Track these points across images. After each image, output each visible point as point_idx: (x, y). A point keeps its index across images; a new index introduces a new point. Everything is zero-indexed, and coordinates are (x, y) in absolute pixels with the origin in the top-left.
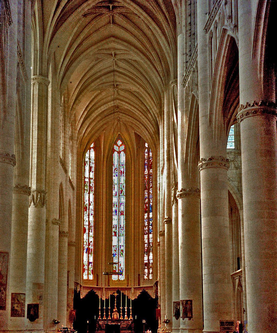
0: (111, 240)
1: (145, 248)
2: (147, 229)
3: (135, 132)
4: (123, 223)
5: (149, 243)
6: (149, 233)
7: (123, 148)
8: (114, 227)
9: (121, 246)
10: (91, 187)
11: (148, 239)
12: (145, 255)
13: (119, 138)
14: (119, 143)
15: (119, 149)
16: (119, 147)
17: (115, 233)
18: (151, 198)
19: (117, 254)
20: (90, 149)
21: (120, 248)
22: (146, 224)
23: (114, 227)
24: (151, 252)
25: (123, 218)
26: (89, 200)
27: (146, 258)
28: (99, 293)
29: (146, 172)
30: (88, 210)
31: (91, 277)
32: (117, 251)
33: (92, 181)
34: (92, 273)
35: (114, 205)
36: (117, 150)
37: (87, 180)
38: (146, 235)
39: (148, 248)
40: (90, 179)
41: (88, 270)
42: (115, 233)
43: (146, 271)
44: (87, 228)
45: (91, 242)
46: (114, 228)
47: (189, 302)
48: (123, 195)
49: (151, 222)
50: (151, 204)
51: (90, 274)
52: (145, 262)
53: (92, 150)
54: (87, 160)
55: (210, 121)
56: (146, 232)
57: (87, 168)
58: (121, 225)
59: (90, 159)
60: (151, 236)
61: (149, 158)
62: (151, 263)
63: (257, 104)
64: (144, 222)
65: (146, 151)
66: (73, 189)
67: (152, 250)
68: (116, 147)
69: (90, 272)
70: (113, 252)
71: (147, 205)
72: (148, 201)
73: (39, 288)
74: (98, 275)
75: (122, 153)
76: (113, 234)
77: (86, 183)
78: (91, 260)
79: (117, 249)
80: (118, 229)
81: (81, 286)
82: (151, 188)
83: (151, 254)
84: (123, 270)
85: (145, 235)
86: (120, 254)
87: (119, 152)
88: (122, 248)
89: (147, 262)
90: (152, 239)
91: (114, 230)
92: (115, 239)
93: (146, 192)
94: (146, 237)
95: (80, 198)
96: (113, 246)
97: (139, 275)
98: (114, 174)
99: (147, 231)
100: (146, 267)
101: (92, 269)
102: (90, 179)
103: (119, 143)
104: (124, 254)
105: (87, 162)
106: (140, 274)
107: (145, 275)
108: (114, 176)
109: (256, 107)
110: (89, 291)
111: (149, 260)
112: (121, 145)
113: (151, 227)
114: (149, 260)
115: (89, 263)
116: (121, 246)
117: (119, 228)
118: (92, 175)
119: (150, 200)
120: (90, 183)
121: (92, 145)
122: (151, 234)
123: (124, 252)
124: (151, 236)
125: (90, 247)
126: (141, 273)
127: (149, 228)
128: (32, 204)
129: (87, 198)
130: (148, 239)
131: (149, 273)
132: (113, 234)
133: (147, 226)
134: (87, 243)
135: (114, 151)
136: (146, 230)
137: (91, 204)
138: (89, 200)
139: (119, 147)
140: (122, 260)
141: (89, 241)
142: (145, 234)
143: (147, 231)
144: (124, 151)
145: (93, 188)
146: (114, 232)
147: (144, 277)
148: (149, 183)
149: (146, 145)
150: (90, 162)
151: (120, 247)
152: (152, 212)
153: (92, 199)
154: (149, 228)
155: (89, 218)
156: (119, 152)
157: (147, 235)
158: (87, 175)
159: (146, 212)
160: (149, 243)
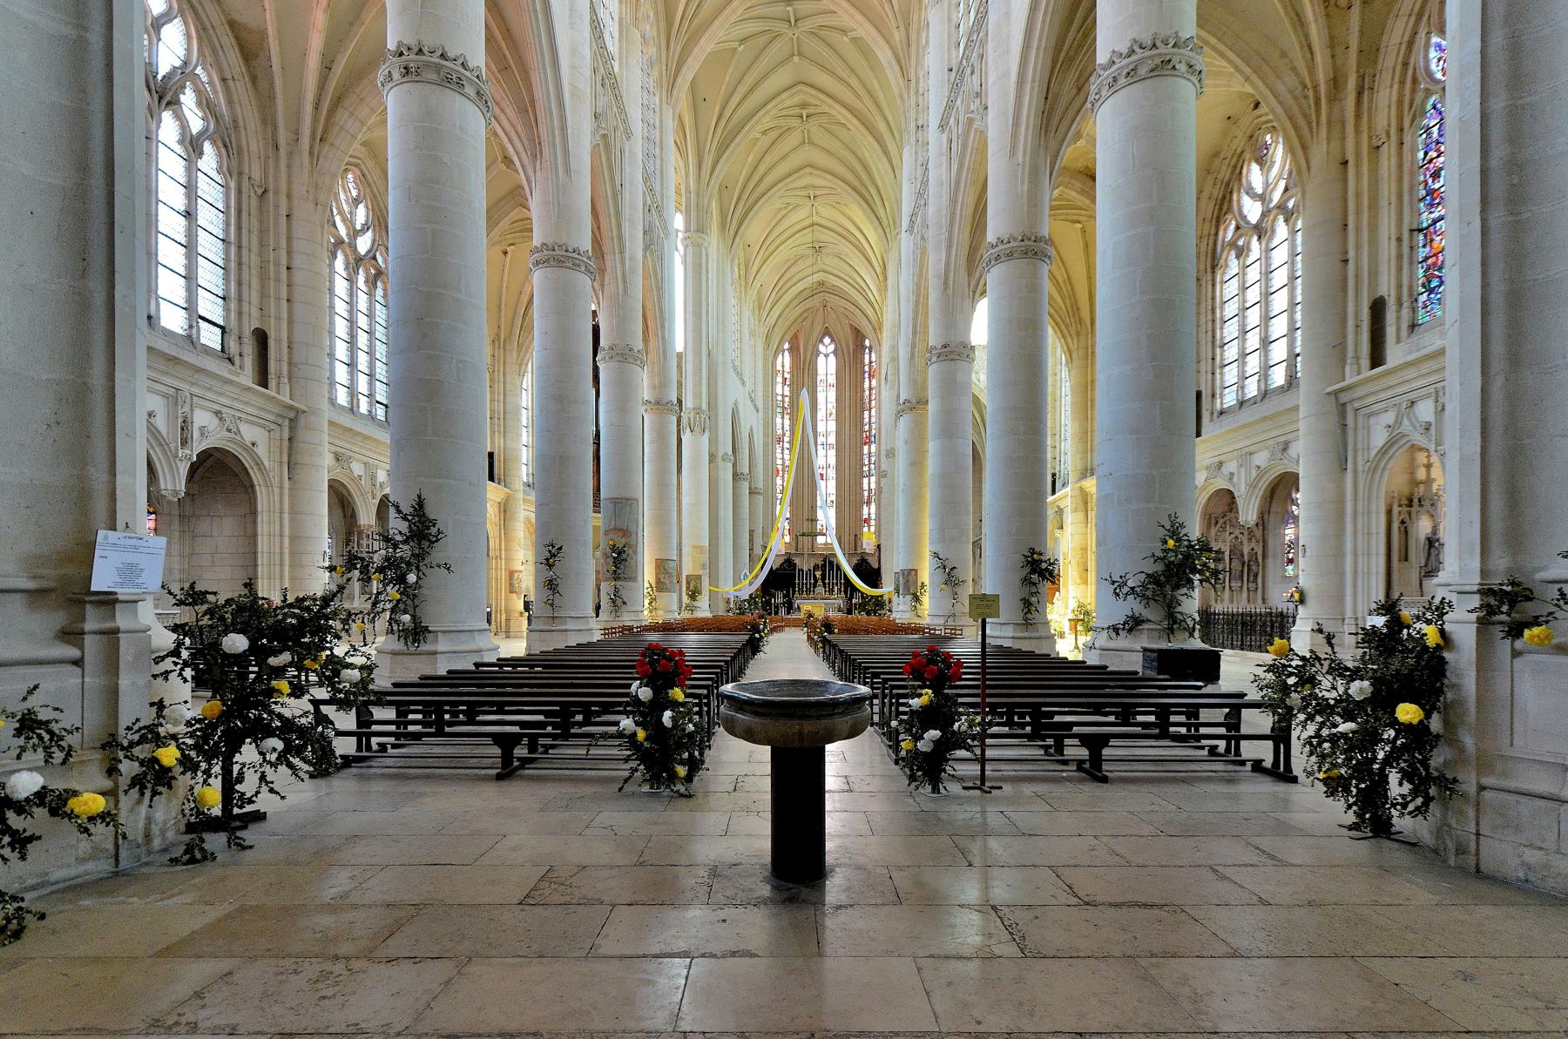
3: (851, 325)
4: (832, 461)
5: (870, 490)
6: (869, 476)
11: (869, 483)
12: (865, 507)
13: (827, 332)
14: (827, 340)
17: (822, 475)
20: (783, 351)
22: (867, 462)
25: (832, 453)
26: (783, 428)
28: (797, 561)
29: (866, 385)
31: (787, 539)
33: (787, 399)
37: (780, 398)
39: (869, 496)
40: (783, 396)
43: (866, 529)
44: (780, 467)
47: (913, 573)
49: (873, 459)
50: (874, 432)
53: (786, 354)
54: (779, 367)
55: (946, 283)
57: (779, 379)
59: (783, 366)
60: (873, 479)
61: (871, 362)
63: (1015, 239)
65: (867, 351)
66: (758, 410)
68: (822, 348)
69: (786, 532)
73: (701, 553)
75: (832, 355)
83: (873, 506)
87: (827, 356)
94: (865, 480)
95: (769, 425)
98: (819, 389)
102: (783, 396)
103: (827, 340)
109: (1013, 244)
111: (869, 514)
114: (869, 514)
118: (787, 392)
120: (783, 401)
121: (786, 346)
124: (873, 479)
126: (858, 533)
128: (688, 429)
129: (779, 426)
130: (869, 483)
135: (818, 353)
138: (783, 428)
140: (832, 513)
148: (870, 401)
149: (867, 343)
153: (787, 427)
156: (827, 356)
158: (779, 389)
160: (870, 490)
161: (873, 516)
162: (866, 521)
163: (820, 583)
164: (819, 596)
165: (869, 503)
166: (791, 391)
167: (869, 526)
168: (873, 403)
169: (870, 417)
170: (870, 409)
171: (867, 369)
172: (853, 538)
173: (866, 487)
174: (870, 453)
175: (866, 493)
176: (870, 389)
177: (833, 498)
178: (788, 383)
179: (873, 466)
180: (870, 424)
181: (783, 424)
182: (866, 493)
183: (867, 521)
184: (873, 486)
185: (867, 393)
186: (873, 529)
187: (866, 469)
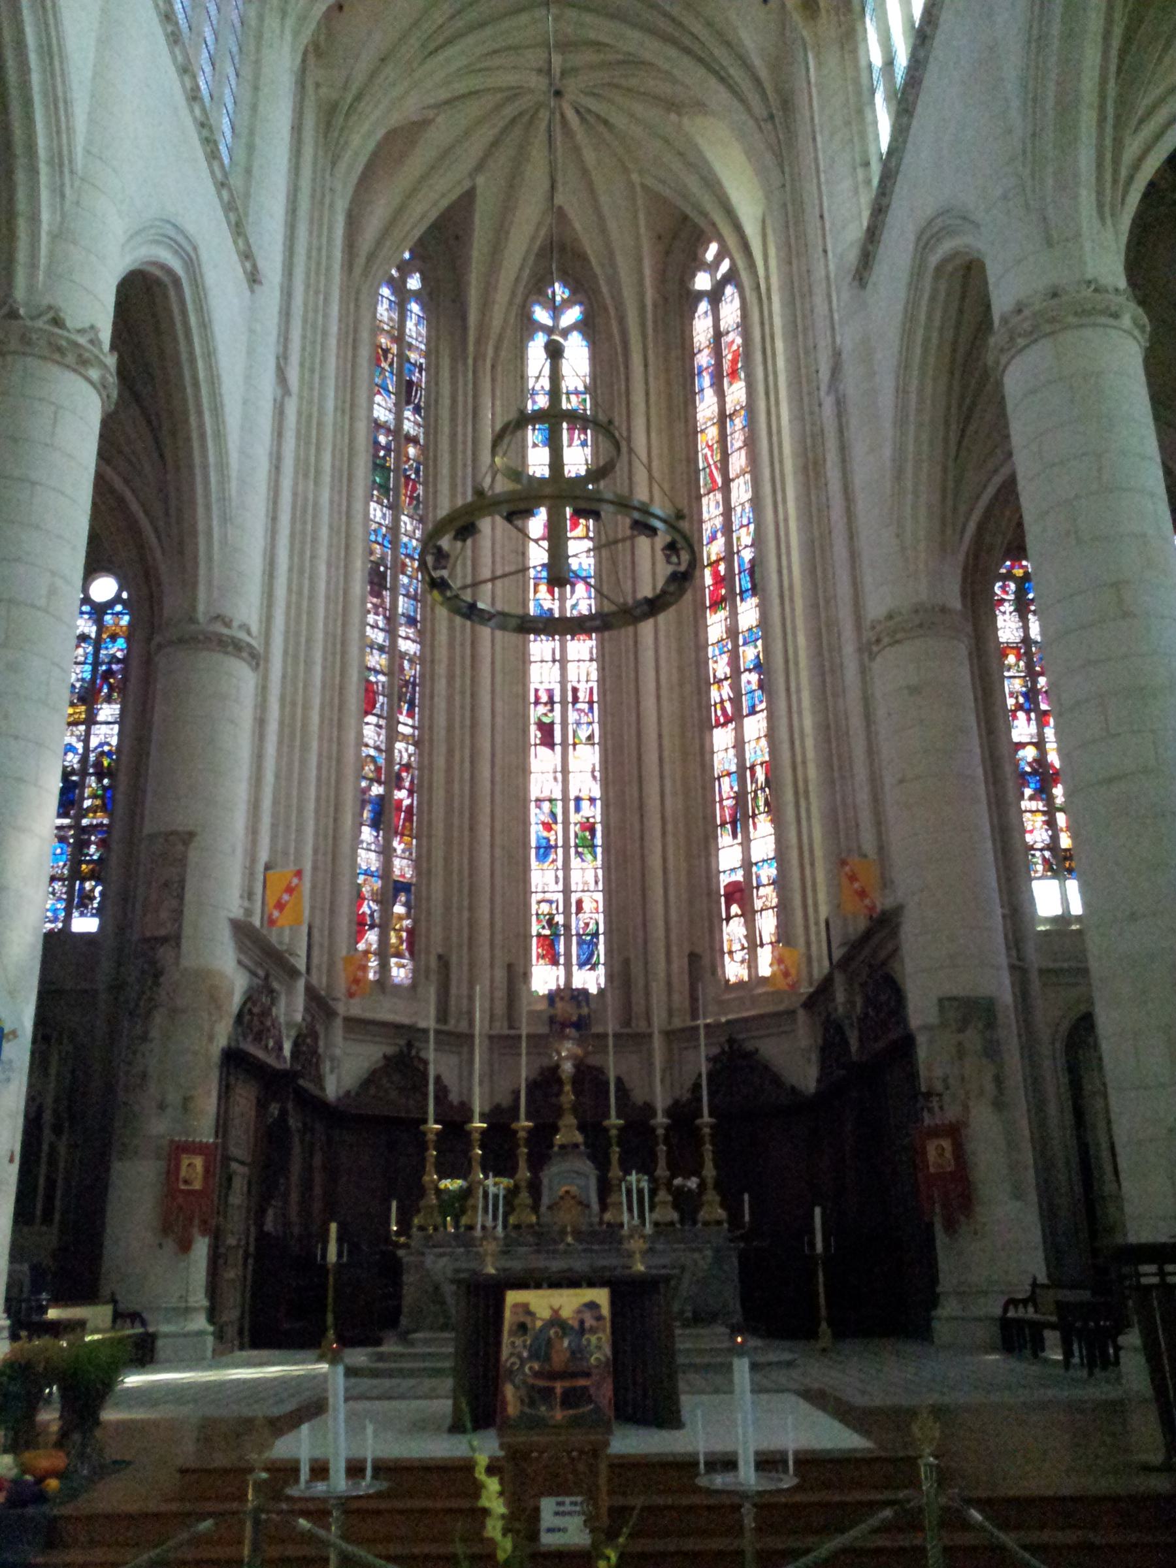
0: (523, 770)
1: (721, 800)
2: (726, 691)
5: (743, 770)
6: (735, 718)
7: (572, 315)
8: (537, 698)
9: (578, 800)
10: (408, 478)
11: (739, 745)
12: (725, 839)
15: (556, 317)
16: (556, 311)
17: (546, 730)
18: (742, 526)
19: (560, 843)
21: (578, 809)
23: (537, 698)
24: (762, 817)
26: (395, 542)
27: (728, 856)
29: (706, 407)
30: (386, 594)
31: (400, 973)
32: (559, 828)
34: (412, 953)
35: (536, 585)
36: (550, 323)
38: (724, 725)
39: (740, 797)
41: (384, 927)
42: (546, 730)
43: (734, 931)
45: (407, 767)
46: (537, 703)
48: (587, 537)
51: (399, 955)
52: (724, 880)
56: (724, 709)
58: (575, 690)
60: (755, 726)
61: (718, 335)
62: (765, 881)
64: (701, 663)
65: (704, 306)
66: (254, 278)
67: (767, 803)
68: (541, 315)
70: (536, 831)
71: (722, 568)
72: (729, 543)
74: (444, 962)
76: (534, 734)
77: (382, 453)
78: (402, 868)
79: (560, 819)
80: (557, 707)
81: (318, 1003)
82: (743, 473)
84: (596, 934)
85: (717, 733)
86: (576, 846)
88: (587, 810)
89: (739, 876)
90: (764, 743)
91: (536, 713)
92: (543, 762)
93: (713, 504)
94: (722, 738)
96: (538, 800)
97: (694, 958)
99: (728, 705)
100: (735, 909)
101: (407, 923)
102: (396, 432)
103: (560, 291)
104: (599, 840)
105: (386, 351)
106: (698, 950)
107: (731, 953)
108: (535, 445)
110: (390, 1050)
112: (568, 303)
113: (754, 677)
114: (747, 864)
115: (393, 889)
116: (578, 800)
117: (564, 703)
119: (738, 539)
122: (753, 712)
123: (599, 834)
125: (401, 795)
127: (736, 687)
130: (739, 745)
131: (753, 943)
132: (534, 734)
133: (726, 679)
134: (378, 769)
135: (529, 327)
136: (722, 702)
137: (409, 570)
139: (556, 311)
141: (390, 759)
142: (718, 725)
143: (728, 705)
144: (586, 327)
145: (420, 490)
146: (541, 725)
147: (723, 966)
148: (725, 456)
150: (402, 358)
151: (572, 804)
152: (754, 595)
154: (736, 687)
155: (392, 633)
157: (731, 726)
159: (716, 605)
161: (768, 872)
162: (741, 893)
163: (568, 1133)
164: (567, 1217)
165: (740, 820)
166: (431, 426)
167: (749, 915)
168: (738, 461)
169: (728, 512)
170: (727, 481)
171: (704, 359)
172: (680, 964)
173: (723, 758)
174: (733, 632)
175: (727, 787)
176: (723, 418)
177: (593, 812)
178: (420, 397)
179: (750, 680)
180: (728, 529)
181: (394, 529)
182: (727, 787)
183: (741, 893)
184: (758, 752)
185: (712, 433)
186: (767, 924)
187: (719, 694)
